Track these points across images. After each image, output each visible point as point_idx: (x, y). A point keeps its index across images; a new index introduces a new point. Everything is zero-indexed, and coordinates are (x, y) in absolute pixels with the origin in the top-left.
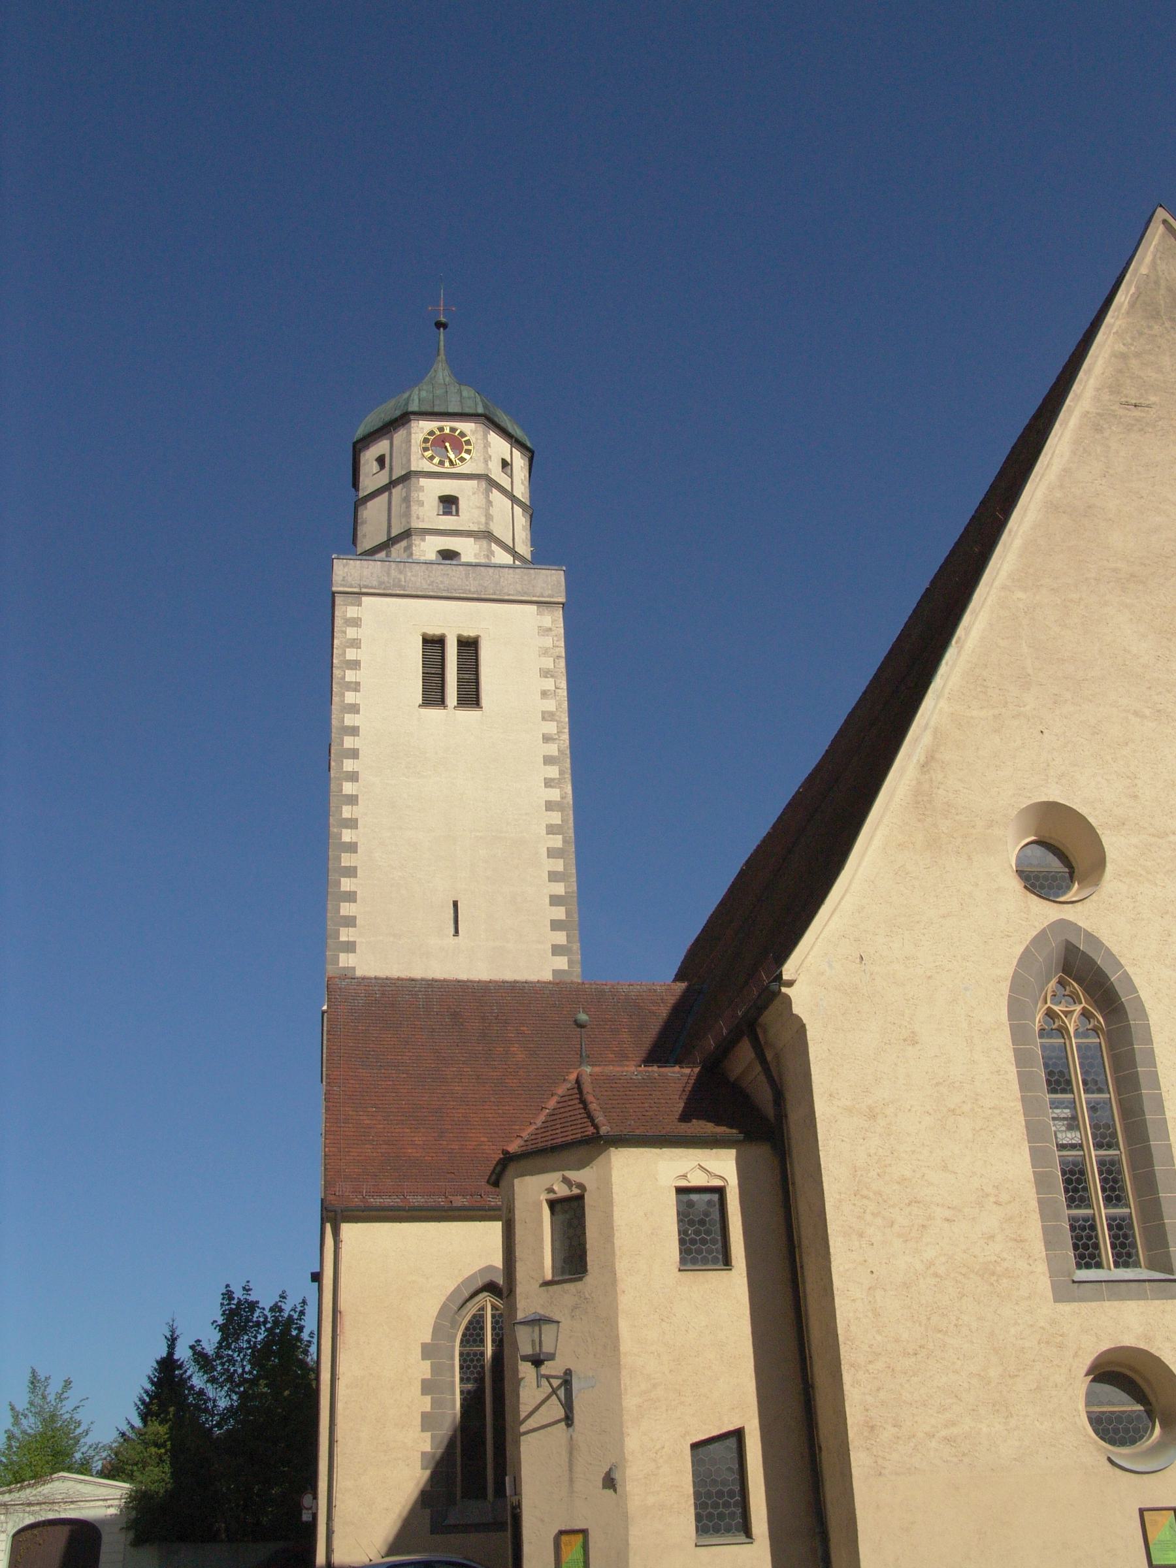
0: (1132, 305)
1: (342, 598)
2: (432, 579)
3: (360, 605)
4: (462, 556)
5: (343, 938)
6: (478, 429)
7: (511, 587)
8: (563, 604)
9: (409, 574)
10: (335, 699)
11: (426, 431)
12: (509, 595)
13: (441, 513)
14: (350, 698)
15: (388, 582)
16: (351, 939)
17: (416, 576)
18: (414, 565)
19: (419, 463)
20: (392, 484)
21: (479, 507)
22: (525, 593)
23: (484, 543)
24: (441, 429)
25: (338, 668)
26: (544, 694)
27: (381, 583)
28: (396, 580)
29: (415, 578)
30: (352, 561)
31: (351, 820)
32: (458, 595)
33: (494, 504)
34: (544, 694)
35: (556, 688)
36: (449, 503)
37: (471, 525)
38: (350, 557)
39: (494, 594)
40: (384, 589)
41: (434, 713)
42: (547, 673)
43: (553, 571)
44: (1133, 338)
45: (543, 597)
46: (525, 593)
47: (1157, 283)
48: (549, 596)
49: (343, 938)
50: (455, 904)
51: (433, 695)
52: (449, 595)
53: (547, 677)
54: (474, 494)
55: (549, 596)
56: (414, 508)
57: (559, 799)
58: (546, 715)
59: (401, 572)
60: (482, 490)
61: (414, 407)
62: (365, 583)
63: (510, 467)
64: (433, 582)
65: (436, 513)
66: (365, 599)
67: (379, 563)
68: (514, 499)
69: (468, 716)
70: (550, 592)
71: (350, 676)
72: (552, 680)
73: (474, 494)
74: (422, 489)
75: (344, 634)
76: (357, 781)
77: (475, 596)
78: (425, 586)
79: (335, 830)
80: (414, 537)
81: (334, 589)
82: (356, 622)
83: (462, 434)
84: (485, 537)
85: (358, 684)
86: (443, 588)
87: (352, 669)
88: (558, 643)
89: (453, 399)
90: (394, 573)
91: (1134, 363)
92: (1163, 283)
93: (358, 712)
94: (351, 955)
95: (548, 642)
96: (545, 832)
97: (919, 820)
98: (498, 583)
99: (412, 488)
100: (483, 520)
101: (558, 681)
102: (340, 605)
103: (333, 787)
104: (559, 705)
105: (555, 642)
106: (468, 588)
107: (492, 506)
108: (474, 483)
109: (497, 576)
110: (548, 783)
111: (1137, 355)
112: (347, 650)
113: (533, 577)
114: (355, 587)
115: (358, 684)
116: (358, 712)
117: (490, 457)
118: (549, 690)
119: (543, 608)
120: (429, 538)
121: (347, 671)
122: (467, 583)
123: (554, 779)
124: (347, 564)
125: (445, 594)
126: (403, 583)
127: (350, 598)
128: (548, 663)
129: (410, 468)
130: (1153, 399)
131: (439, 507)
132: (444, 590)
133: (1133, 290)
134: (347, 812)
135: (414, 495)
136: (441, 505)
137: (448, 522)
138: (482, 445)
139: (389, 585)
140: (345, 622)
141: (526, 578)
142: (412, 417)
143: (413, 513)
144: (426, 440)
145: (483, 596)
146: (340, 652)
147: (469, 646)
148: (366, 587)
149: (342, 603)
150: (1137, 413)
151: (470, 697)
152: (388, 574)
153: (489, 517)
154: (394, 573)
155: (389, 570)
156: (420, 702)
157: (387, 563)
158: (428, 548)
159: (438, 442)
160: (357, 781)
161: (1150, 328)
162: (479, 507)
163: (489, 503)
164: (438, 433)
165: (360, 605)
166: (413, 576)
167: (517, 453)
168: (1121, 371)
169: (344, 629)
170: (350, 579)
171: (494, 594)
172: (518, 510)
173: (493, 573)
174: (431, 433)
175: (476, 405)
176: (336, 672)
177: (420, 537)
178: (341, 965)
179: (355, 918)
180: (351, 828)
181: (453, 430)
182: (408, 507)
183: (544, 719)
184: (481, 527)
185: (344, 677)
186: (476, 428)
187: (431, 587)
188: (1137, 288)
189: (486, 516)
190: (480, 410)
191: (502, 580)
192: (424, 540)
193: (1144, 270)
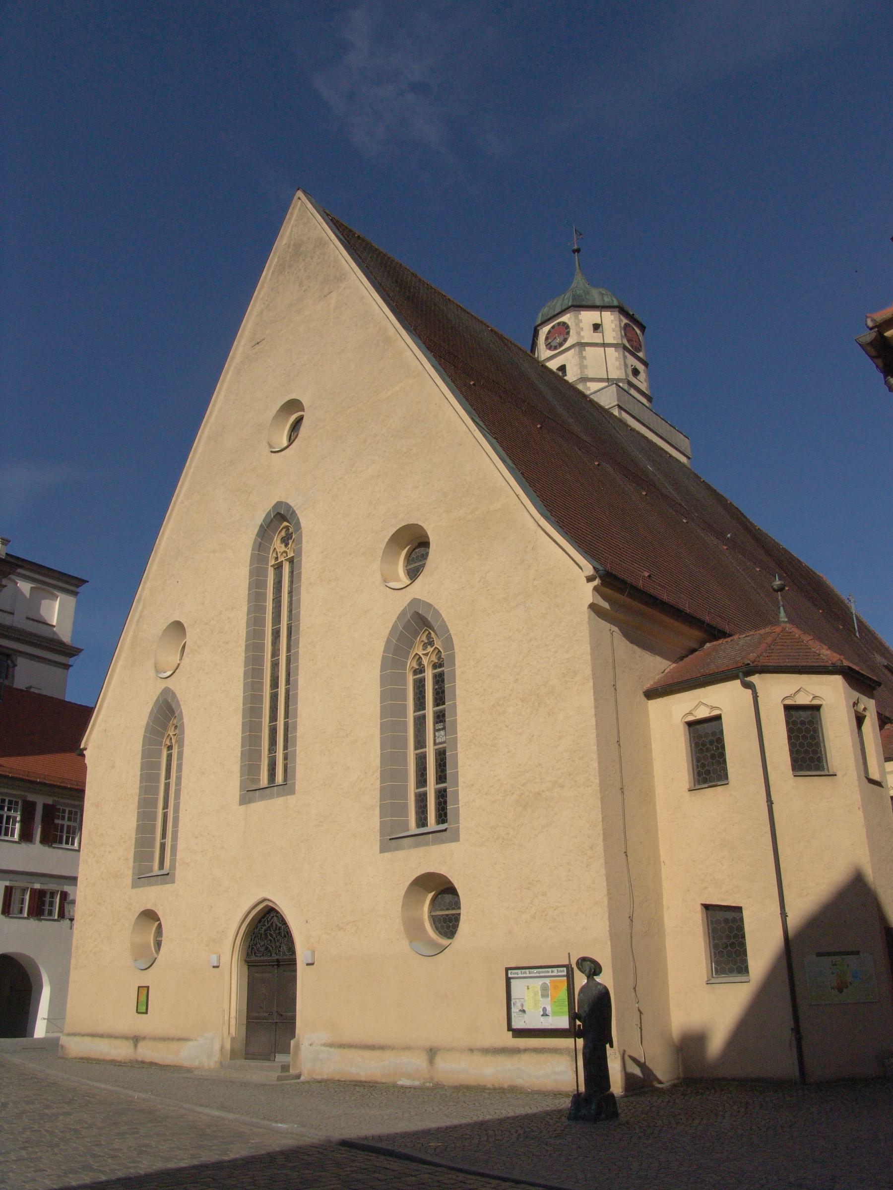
8: (618, 405)
21: (576, 365)
48: (609, 405)
54: (573, 357)
73: (573, 357)
100: (579, 371)
107: (586, 359)
117: (582, 329)
138: (575, 325)
142: (538, 328)
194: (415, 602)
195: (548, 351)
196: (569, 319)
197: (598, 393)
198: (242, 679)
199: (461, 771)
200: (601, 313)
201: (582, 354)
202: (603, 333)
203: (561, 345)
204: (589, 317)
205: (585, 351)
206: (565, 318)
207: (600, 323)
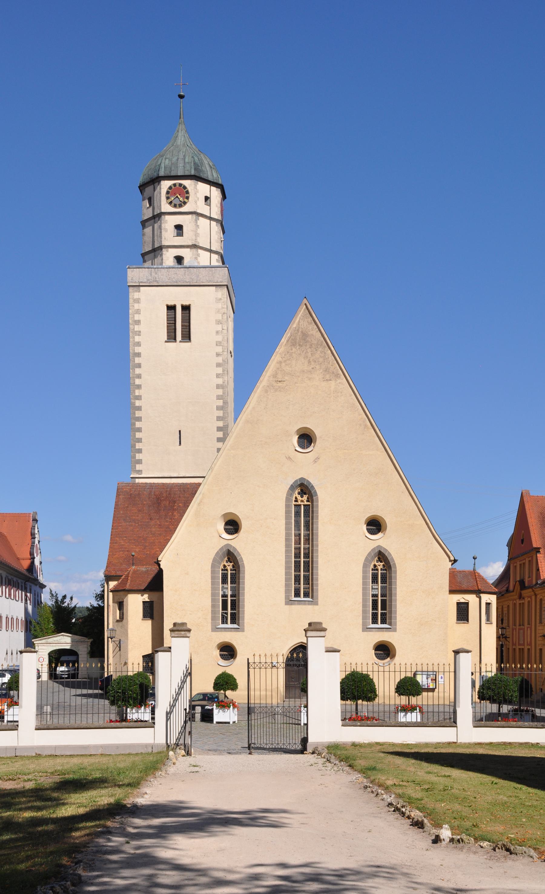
0: (288, 341)
1: (132, 289)
2: (170, 276)
3: (139, 292)
4: (185, 259)
5: (137, 447)
6: (192, 183)
7: (204, 278)
9: (160, 274)
10: (131, 340)
11: (168, 187)
12: (205, 282)
13: (175, 235)
14: (137, 339)
15: (151, 279)
16: (140, 448)
17: (163, 275)
18: (162, 269)
19: (166, 207)
21: (192, 231)
23: (194, 250)
24: (175, 185)
25: (131, 324)
26: (217, 332)
27: (148, 280)
28: (155, 278)
29: (163, 276)
30: (135, 269)
31: (139, 396)
32: (181, 284)
33: (200, 226)
34: (217, 332)
35: (223, 329)
36: (179, 228)
37: (189, 241)
38: (134, 266)
39: (197, 282)
40: (149, 283)
41: (172, 345)
42: (219, 322)
43: (223, 268)
44: (285, 355)
45: (218, 282)
47: (298, 330)
48: (221, 282)
49: (137, 447)
50: (180, 431)
51: (172, 337)
52: (177, 284)
53: (219, 324)
54: (190, 223)
55: (221, 282)
56: (163, 233)
57: (222, 383)
58: (218, 343)
59: (156, 274)
60: (193, 220)
61: (162, 173)
62: (141, 281)
63: (209, 199)
64: (170, 278)
65: (173, 236)
66: (142, 288)
67: (147, 269)
68: (211, 219)
70: (221, 280)
71: (137, 328)
72: (221, 325)
73: (190, 223)
74: (166, 222)
75: (133, 307)
76: (141, 378)
77: (188, 284)
78: (167, 280)
79: (133, 401)
80: (163, 250)
81: (128, 284)
82: (138, 301)
83: (185, 188)
84: (195, 248)
85: (140, 332)
86: (174, 281)
87: (137, 325)
88: (223, 306)
89: (181, 165)
90: (153, 274)
91: (283, 364)
92: (300, 330)
93: (140, 346)
94: (140, 454)
95: (220, 306)
96: (216, 399)
97: (196, 519)
98: (198, 276)
99: (162, 222)
100: (194, 238)
101: (223, 326)
102: (131, 292)
103: (131, 381)
105: (223, 306)
106: (185, 280)
107: (199, 228)
108: (190, 216)
109: (198, 273)
110: (218, 376)
111: (285, 361)
112: (135, 315)
113: (214, 272)
114: (137, 283)
115: (140, 332)
116: (140, 346)
118: (219, 331)
119: (218, 288)
120: (170, 250)
121: (135, 326)
122: (185, 277)
123: (220, 374)
124: (133, 271)
125: (175, 284)
126: (157, 279)
127: (135, 288)
129: (161, 209)
130: (286, 378)
131: (174, 231)
132: (175, 282)
133: (289, 335)
134: (137, 392)
135: (163, 225)
136: (176, 230)
137: (178, 241)
138: (194, 193)
139: (151, 281)
140: (134, 301)
141: (210, 272)
143: (162, 236)
144: (168, 193)
145: (192, 284)
146: (132, 317)
147: (186, 309)
148: (142, 282)
149: (132, 291)
150: (280, 384)
151: (187, 336)
153: (197, 235)
154: (153, 274)
155: (151, 272)
156: (166, 339)
157: (150, 269)
158: (169, 257)
160: (141, 378)
161: (292, 349)
162: (192, 231)
163: (198, 226)
164: (173, 187)
165: (139, 292)
166: (161, 275)
167: (214, 189)
168: (278, 369)
169: (133, 304)
170: (134, 278)
171: (197, 282)
173: (196, 271)
174: (170, 188)
175: (191, 168)
177: (166, 250)
178: (137, 458)
179: (141, 439)
180: (139, 400)
181: (180, 185)
182: (161, 232)
183: (217, 345)
184: (193, 242)
185: (134, 329)
186: (191, 182)
187: (169, 281)
188: (291, 333)
189: (195, 235)
190: (193, 173)
191: (200, 275)
192: (167, 251)
193: (295, 326)
194: (379, 546)
197: (213, 269)
198: (284, 552)
199: (398, 610)
200: (210, 187)
201: (197, 223)
202: (210, 206)
203: (180, 206)
204: (203, 189)
205: (199, 220)
206: (186, 183)
207: (209, 197)
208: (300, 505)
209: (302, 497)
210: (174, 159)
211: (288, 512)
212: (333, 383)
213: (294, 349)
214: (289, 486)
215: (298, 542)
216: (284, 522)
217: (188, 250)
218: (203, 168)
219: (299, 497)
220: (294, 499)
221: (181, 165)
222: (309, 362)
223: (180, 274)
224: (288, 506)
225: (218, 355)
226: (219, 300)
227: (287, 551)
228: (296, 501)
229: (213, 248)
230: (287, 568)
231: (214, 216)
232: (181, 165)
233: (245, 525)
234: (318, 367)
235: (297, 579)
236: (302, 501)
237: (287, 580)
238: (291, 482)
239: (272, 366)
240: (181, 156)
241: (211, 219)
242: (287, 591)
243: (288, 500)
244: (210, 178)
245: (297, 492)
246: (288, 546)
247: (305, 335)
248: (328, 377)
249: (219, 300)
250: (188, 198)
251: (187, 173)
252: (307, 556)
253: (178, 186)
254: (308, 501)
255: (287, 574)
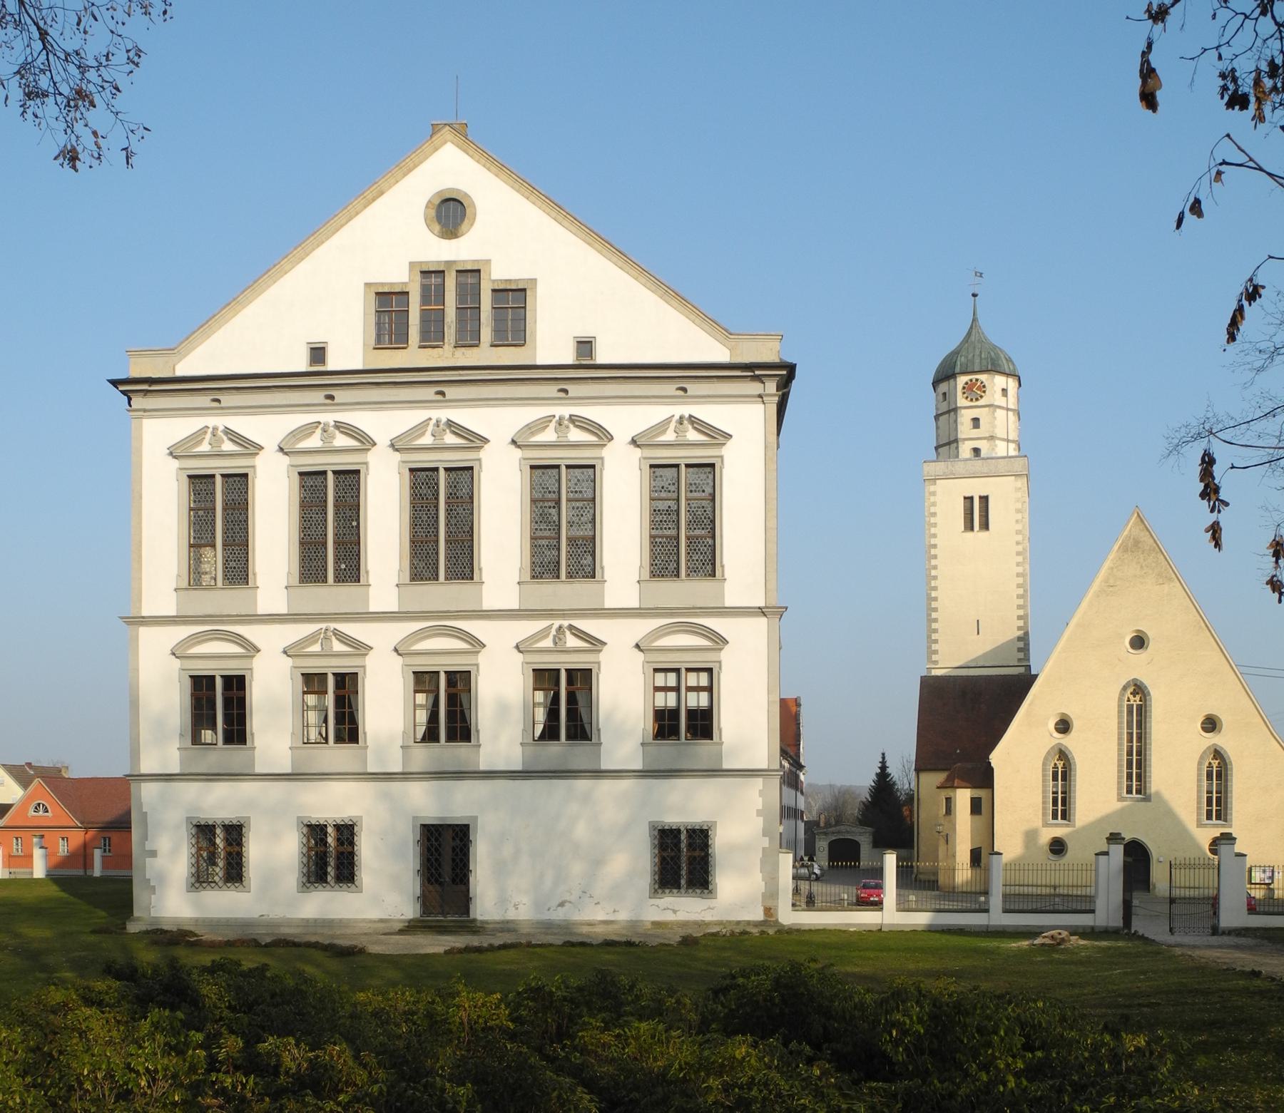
0: (1119, 548)
11: (964, 382)
20: (949, 412)
22: (1009, 471)
24: (971, 380)
26: (1017, 521)
29: (959, 467)
34: (1017, 521)
36: (976, 422)
41: (969, 534)
46: (1009, 471)
51: (969, 526)
56: (959, 427)
66: (938, 481)
68: (1008, 409)
69: (984, 534)
74: (962, 416)
82: (934, 494)
90: (950, 467)
91: (1115, 570)
104: (1023, 527)
108: (987, 409)
110: (1018, 564)
115: (936, 524)
120: (966, 442)
128: (1019, 506)
135: (959, 420)
144: (964, 388)
147: (985, 500)
150: (1111, 589)
151: (985, 525)
152: (947, 467)
153: (994, 426)
154: (950, 467)
156: (963, 529)
159: (968, 387)
163: (995, 418)
172: (1010, 413)
174: (966, 383)
176: (927, 519)
195: (964, 400)
196: (988, 379)
206: (983, 377)
208: (1133, 705)
209: (1135, 697)
210: (970, 356)
211: (1120, 712)
212: (1166, 587)
213: (1126, 556)
214: (1122, 687)
215: (1130, 740)
216: (1116, 721)
217: (985, 441)
218: (1000, 362)
219: (1131, 697)
220: (1126, 699)
221: (977, 361)
222: (1142, 567)
223: (978, 465)
224: (1120, 706)
225: (1018, 543)
226: (1018, 489)
227: (1120, 750)
228: (1129, 700)
229: (1010, 438)
230: (1120, 766)
231: (1011, 406)
232: (977, 361)
233: (1076, 725)
234: (1151, 572)
235: (1129, 777)
236: (1135, 701)
237: (1120, 777)
238: (1124, 683)
239: (1103, 571)
240: (977, 352)
241: (1008, 409)
242: (1119, 788)
243: (1120, 700)
244: (1007, 371)
245: (1129, 692)
246: (1120, 744)
247: (1137, 543)
248: (1161, 581)
249: (1018, 489)
250: (984, 392)
251: (984, 368)
252: (1139, 754)
253: (974, 381)
254: (1140, 701)
255: (1120, 771)
